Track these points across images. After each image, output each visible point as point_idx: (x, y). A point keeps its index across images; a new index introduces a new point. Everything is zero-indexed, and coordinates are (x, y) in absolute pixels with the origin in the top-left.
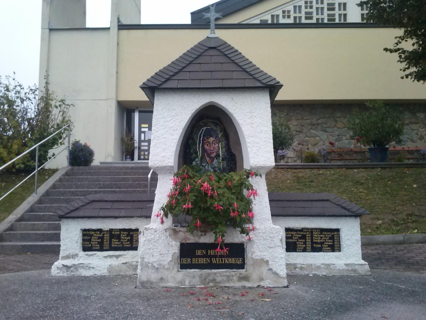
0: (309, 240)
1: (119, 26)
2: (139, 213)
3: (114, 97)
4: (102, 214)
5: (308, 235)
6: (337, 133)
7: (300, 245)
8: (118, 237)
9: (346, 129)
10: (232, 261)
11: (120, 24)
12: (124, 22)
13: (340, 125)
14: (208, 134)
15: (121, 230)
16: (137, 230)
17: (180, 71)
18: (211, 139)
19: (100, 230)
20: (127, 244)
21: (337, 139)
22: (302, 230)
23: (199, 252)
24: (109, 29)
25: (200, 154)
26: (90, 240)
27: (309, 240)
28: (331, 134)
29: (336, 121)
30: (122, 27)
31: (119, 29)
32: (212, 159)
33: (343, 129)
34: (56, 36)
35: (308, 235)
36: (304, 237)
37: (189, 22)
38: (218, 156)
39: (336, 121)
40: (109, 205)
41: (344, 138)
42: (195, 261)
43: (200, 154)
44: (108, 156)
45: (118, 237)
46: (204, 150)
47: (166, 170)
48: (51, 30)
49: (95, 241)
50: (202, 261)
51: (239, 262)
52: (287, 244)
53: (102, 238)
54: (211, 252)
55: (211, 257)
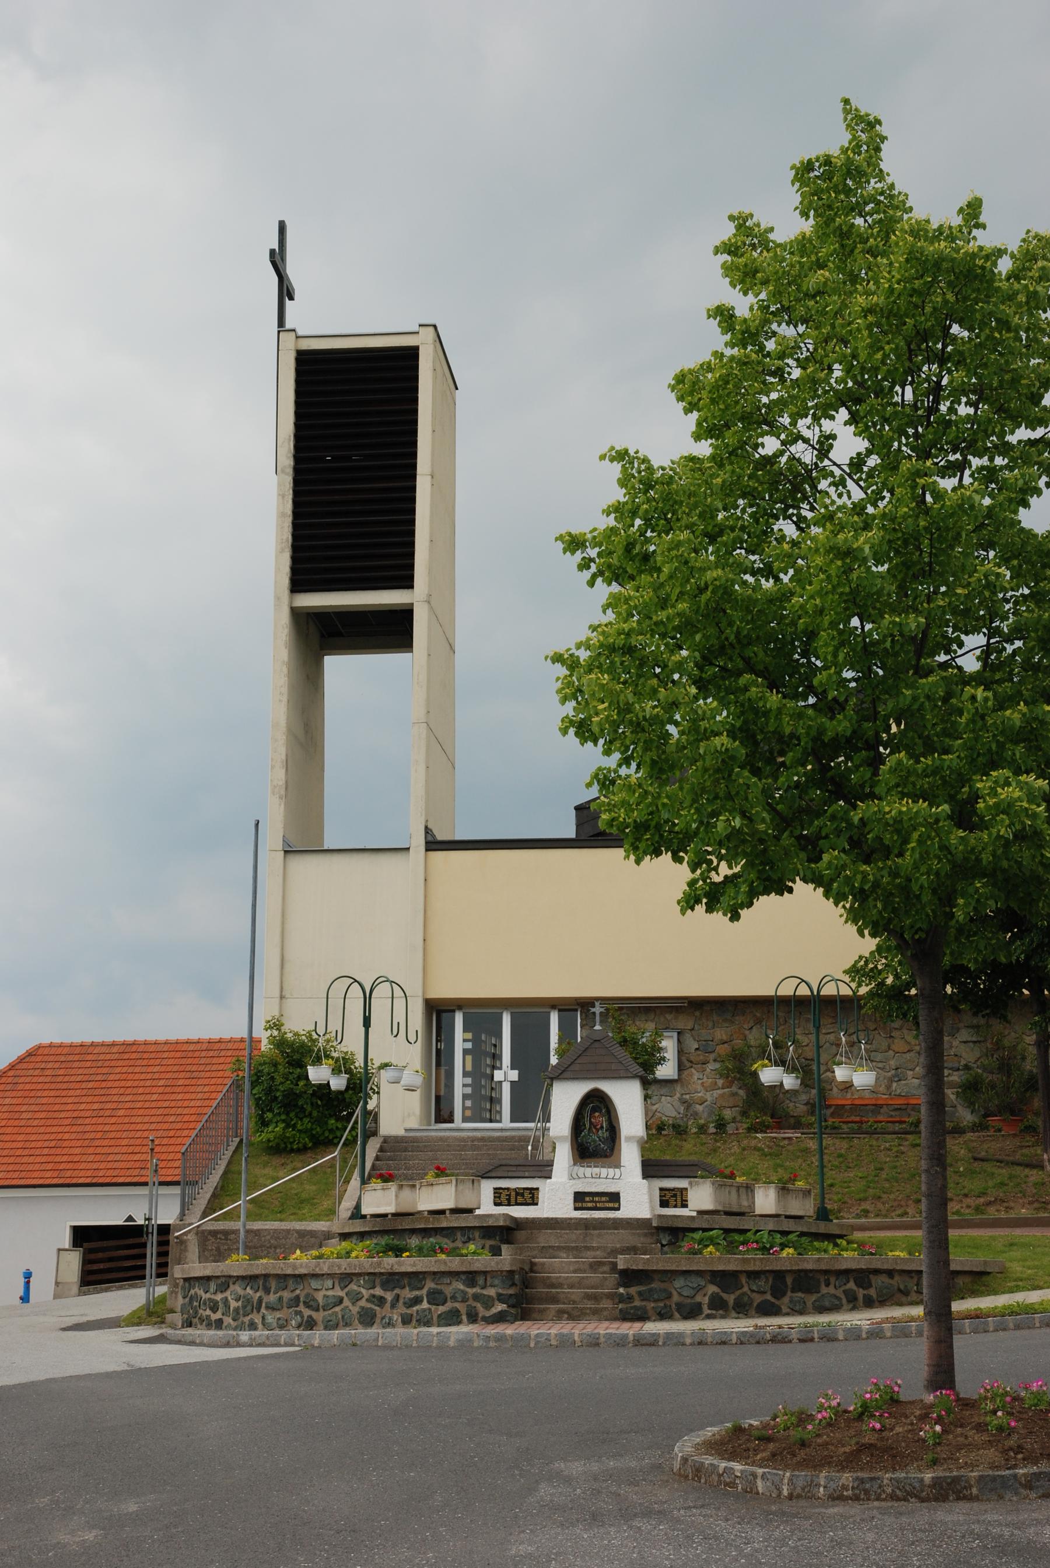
0: (679, 1199)
1: (427, 843)
2: (540, 1174)
3: (420, 994)
4: (510, 1174)
5: (679, 1194)
6: (893, 1063)
7: (672, 1202)
8: (522, 1195)
9: (912, 1054)
10: (611, 1205)
11: (430, 838)
12: (440, 836)
13: (899, 1045)
14: (594, 1110)
15: (524, 1189)
16: (537, 1189)
17: (572, 1063)
18: (597, 1114)
19: (508, 1189)
20: (529, 1201)
21: (894, 1076)
22: (673, 1190)
23: (587, 1199)
24: (408, 849)
25: (587, 1126)
26: (499, 1197)
27: (679, 1199)
28: (880, 1065)
29: (891, 1037)
30: (433, 845)
31: (427, 850)
32: (598, 1130)
33: (908, 1056)
34: (290, 857)
35: (679, 1194)
36: (675, 1196)
37: (571, 833)
38: (602, 1127)
39: (891, 1037)
40: (514, 1169)
41: (910, 1073)
42: (584, 1205)
43: (587, 1126)
44: (409, 1115)
45: (522, 1195)
46: (591, 1122)
47: (562, 1138)
48: (286, 852)
49: (504, 1198)
50: (590, 1205)
51: (616, 1206)
52: (661, 1201)
53: (509, 1195)
54: (596, 1199)
55: (596, 1202)
